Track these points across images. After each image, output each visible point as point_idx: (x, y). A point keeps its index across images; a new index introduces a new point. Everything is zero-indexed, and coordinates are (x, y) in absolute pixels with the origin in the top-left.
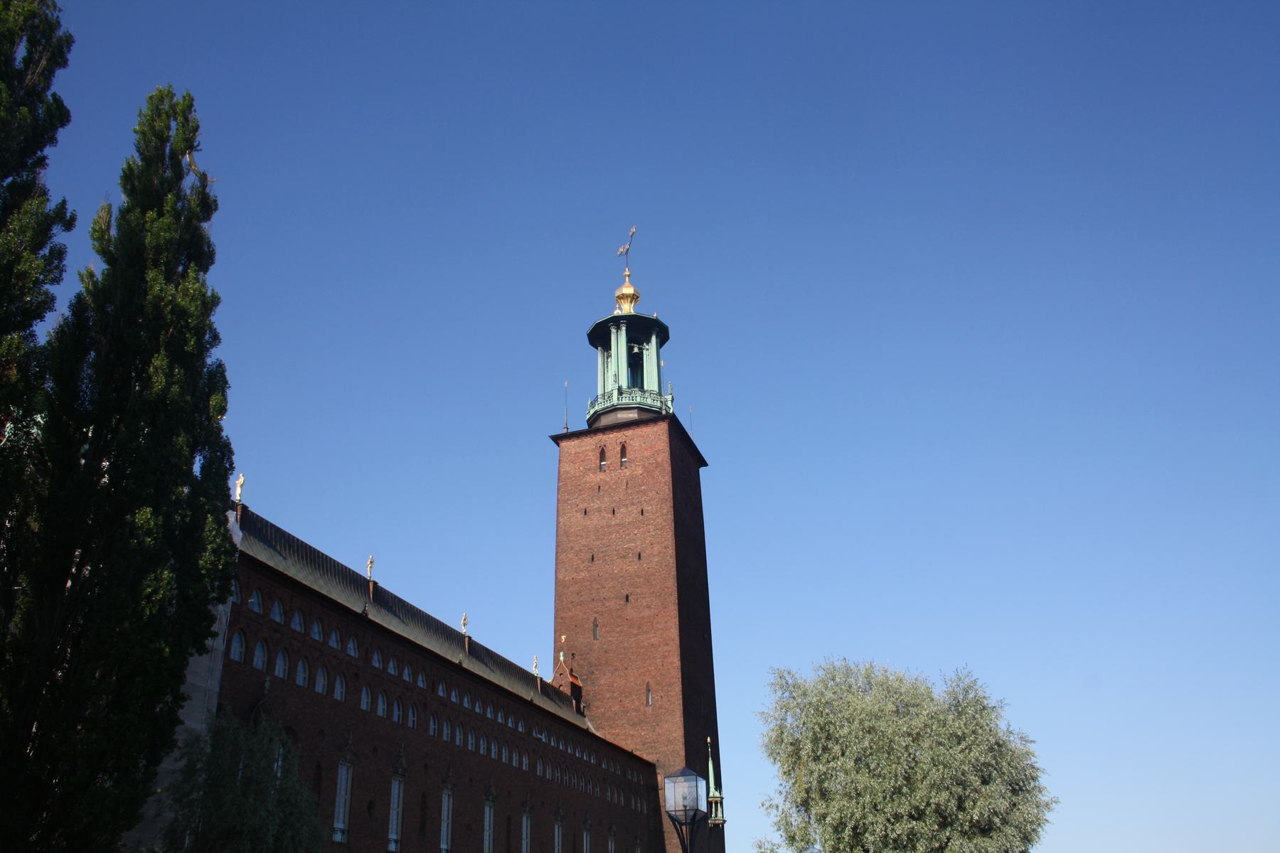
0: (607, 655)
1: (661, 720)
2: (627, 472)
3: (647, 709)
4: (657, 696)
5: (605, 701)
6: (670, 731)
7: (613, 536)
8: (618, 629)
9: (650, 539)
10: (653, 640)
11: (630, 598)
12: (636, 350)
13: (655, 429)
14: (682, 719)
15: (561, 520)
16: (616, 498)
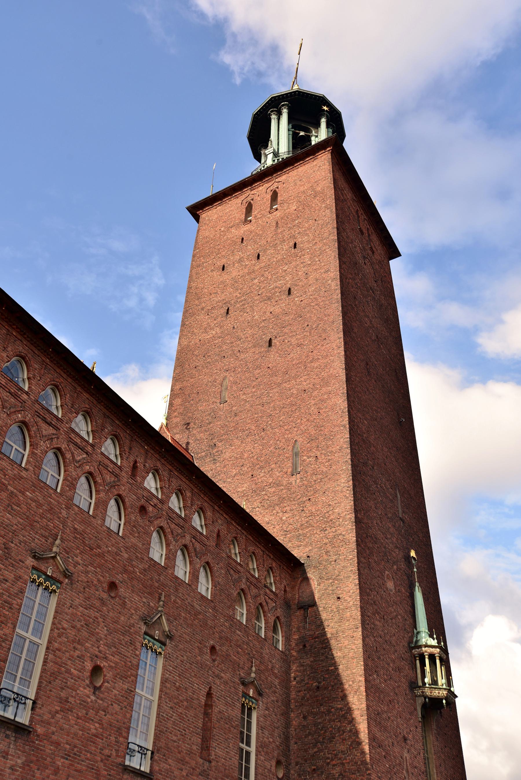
0: (237, 418)
1: (316, 491)
2: (278, 214)
3: (292, 479)
4: (309, 457)
5: (229, 480)
6: (330, 505)
7: (256, 281)
8: (254, 383)
9: (304, 269)
10: (305, 383)
11: (273, 341)
12: (302, 133)
13: (315, 163)
14: (351, 483)
15: (193, 285)
16: (263, 242)
